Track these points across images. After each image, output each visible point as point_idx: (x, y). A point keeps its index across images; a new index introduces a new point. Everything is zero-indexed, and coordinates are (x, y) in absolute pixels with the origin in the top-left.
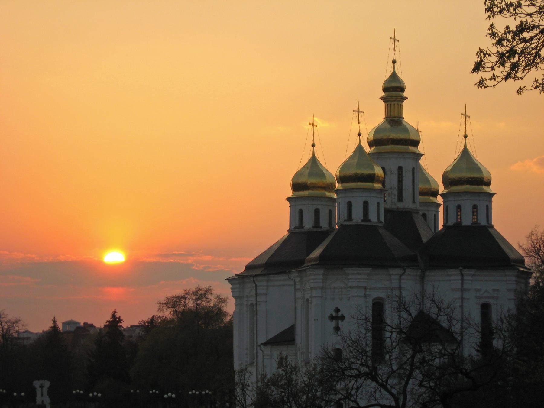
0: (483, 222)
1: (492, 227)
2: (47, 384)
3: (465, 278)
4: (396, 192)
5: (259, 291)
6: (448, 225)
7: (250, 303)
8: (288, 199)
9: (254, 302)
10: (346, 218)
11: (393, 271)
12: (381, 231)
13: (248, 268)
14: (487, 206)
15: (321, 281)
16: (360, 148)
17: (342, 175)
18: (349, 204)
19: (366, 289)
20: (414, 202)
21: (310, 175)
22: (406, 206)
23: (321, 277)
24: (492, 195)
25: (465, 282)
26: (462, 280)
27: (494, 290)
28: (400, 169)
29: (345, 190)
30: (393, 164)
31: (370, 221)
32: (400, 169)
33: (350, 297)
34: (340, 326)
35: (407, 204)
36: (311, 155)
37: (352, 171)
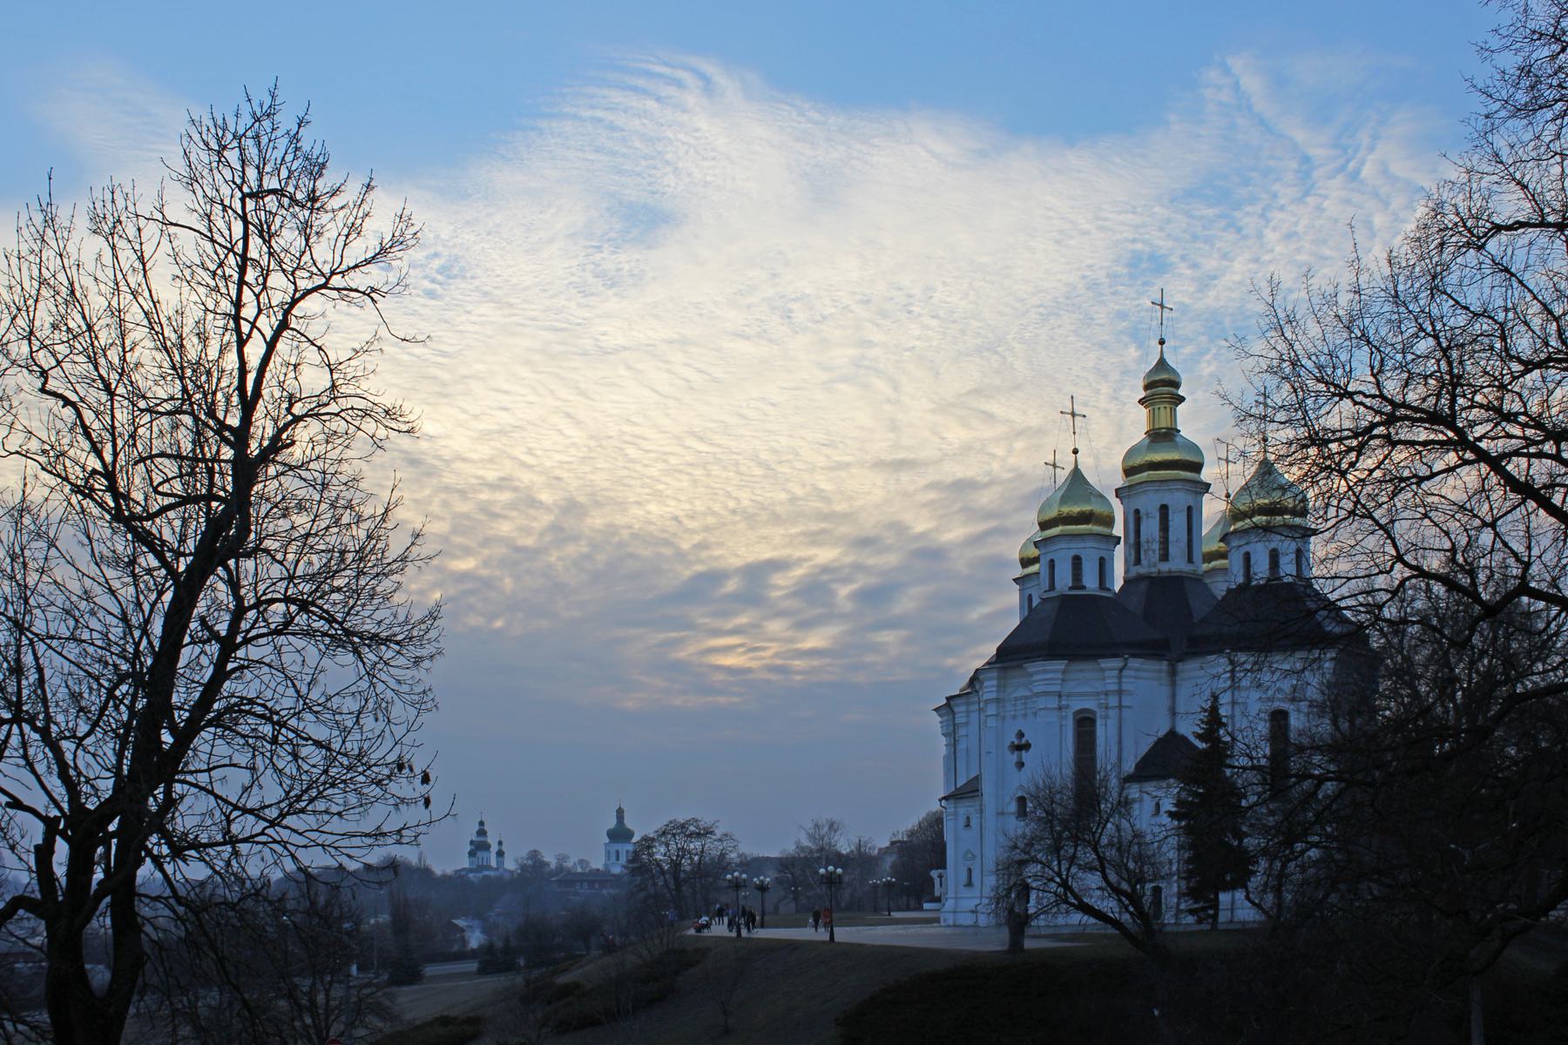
4: (1156, 546)
15: (994, 689)
19: (1060, 696)
22: (1174, 568)
23: (995, 682)
28: (1164, 509)
30: (1149, 503)
31: (1083, 588)
32: (1164, 509)
34: (1024, 760)
35: (1177, 564)
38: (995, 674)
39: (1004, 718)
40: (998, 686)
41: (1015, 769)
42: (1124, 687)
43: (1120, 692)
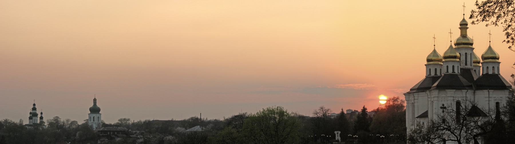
0: (496, 73)
1: (500, 74)
2: (339, 132)
3: (490, 93)
4: (464, 62)
5: (415, 98)
6: (484, 74)
7: (412, 102)
8: (425, 65)
9: (413, 102)
11: (463, 91)
12: (459, 76)
13: (411, 90)
14: (498, 67)
16: (451, 46)
17: (445, 56)
18: (447, 67)
19: (453, 97)
20: (471, 65)
21: (433, 56)
22: (468, 67)
23: (437, 93)
24: (499, 63)
25: (490, 94)
26: (489, 94)
27: (501, 97)
28: (466, 54)
29: (446, 61)
30: (463, 52)
31: (455, 73)
32: (466, 54)
35: (468, 66)
36: (434, 49)
37: (449, 54)
39: (439, 101)
42: (467, 96)
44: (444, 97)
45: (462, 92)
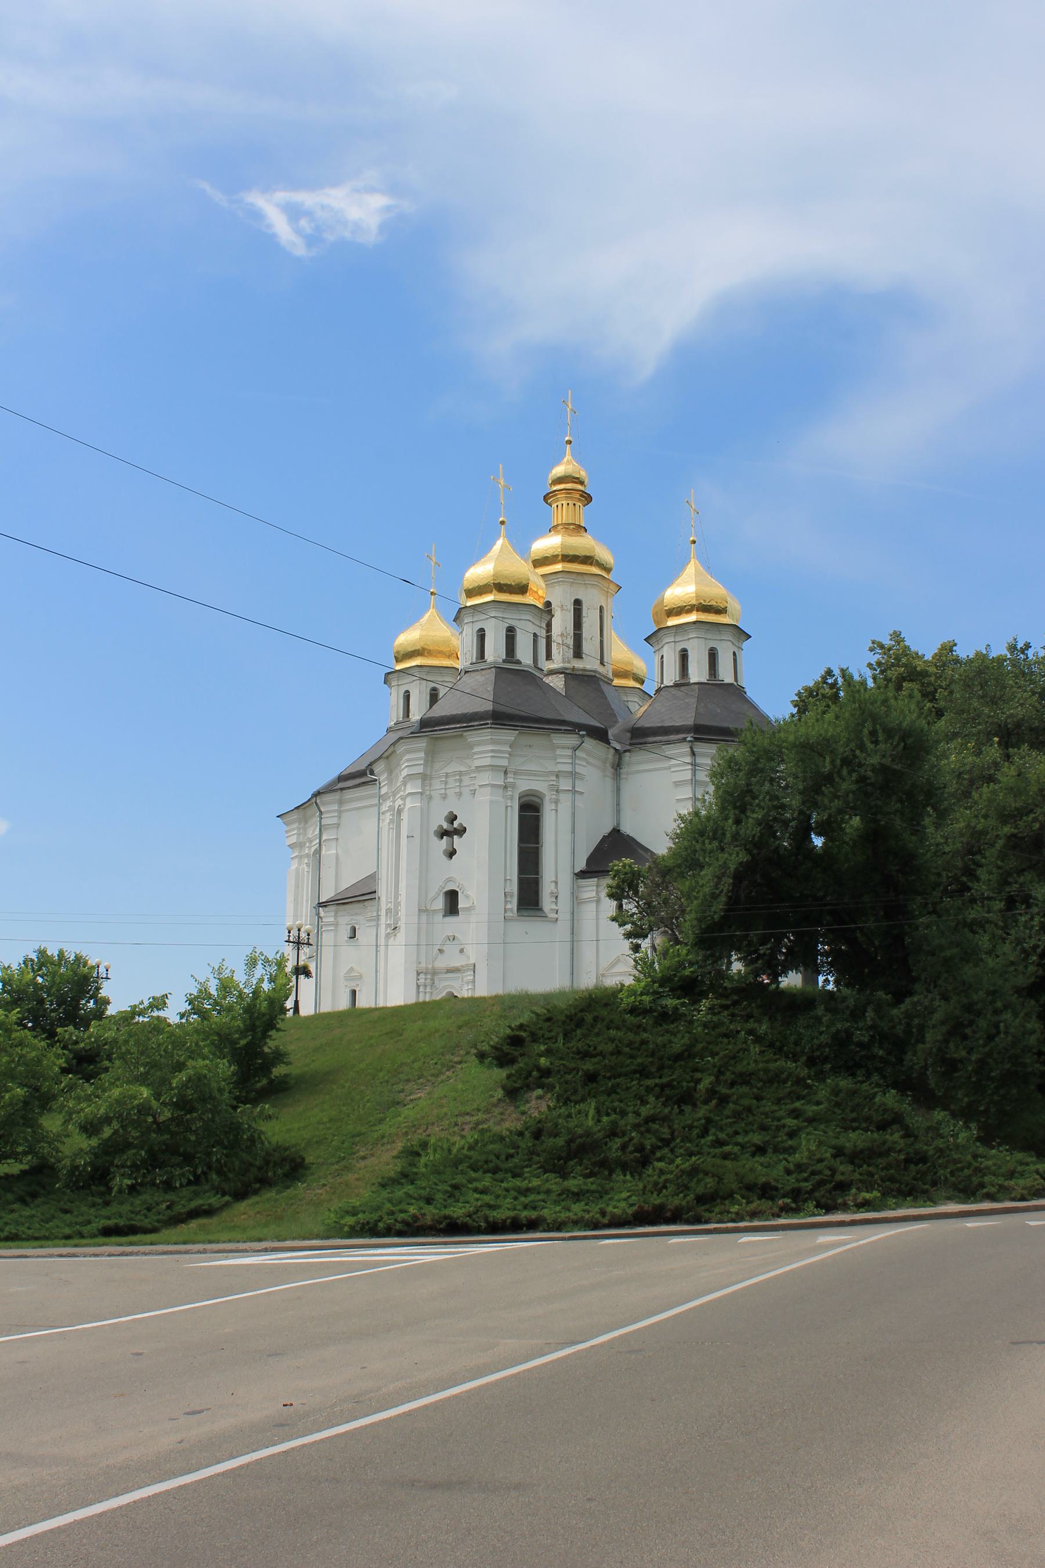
4: (570, 641)
10: (474, 660)
15: (422, 762)
19: (506, 772)
22: (588, 667)
23: (422, 755)
31: (519, 662)
32: (578, 603)
33: (476, 790)
38: (422, 743)
39: (430, 798)
40: (426, 761)
41: (445, 858)
42: (578, 769)
43: (574, 775)
44: (455, 773)
45: (554, 748)
